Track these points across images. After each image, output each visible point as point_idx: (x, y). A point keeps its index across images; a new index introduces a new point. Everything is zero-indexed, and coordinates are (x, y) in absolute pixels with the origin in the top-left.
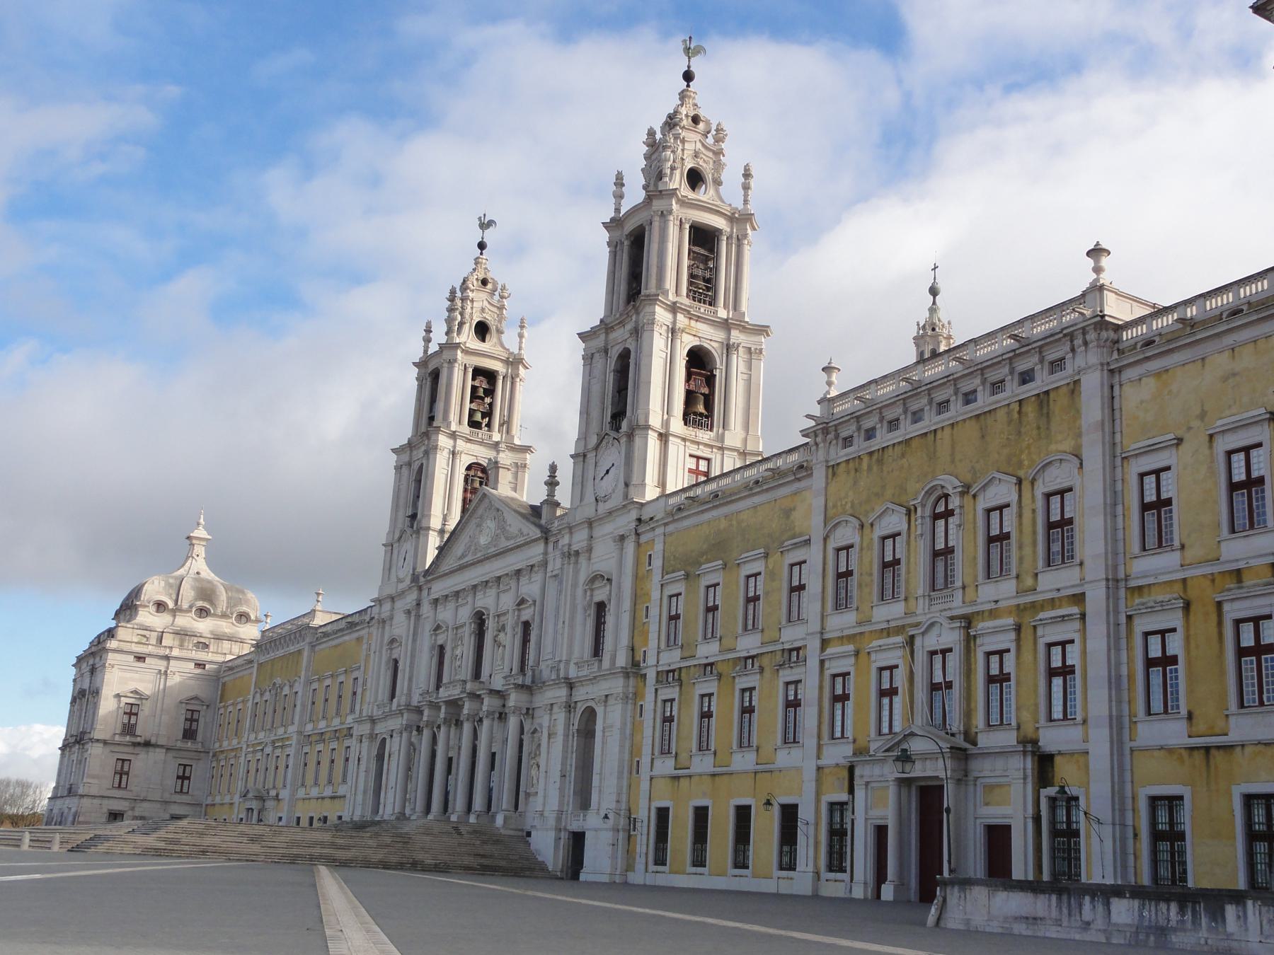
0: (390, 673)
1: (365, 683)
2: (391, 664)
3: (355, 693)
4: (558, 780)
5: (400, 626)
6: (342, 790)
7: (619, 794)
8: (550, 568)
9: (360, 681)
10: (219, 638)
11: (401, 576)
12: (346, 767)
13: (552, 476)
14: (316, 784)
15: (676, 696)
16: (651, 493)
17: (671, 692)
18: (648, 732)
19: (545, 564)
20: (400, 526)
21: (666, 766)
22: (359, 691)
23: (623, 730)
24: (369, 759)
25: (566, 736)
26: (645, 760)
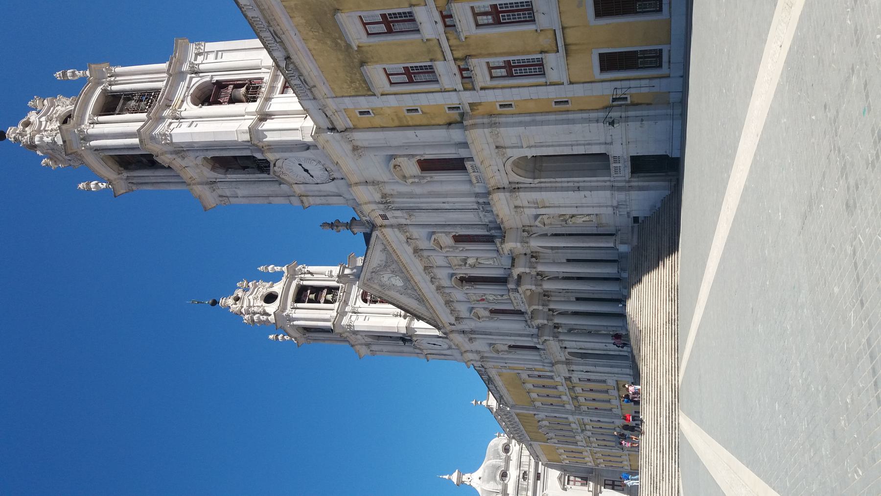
0: (519, 351)
1: (530, 369)
2: (512, 350)
3: (539, 376)
4: (582, 193)
5: (480, 345)
6: (611, 382)
7: (590, 121)
8: (403, 221)
9: (530, 373)
10: (520, 465)
11: (446, 346)
12: (594, 381)
13: (332, 225)
14: (609, 401)
15: (483, 61)
16: (309, 123)
17: (479, 69)
18: (525, 93)
19: (400, 226)
20: (411, 349)
21: (554, 63)
22: (536, 373)
23: (526, 124)
24: (586, 365)
25: (541, 189)
26: (553, 93)
